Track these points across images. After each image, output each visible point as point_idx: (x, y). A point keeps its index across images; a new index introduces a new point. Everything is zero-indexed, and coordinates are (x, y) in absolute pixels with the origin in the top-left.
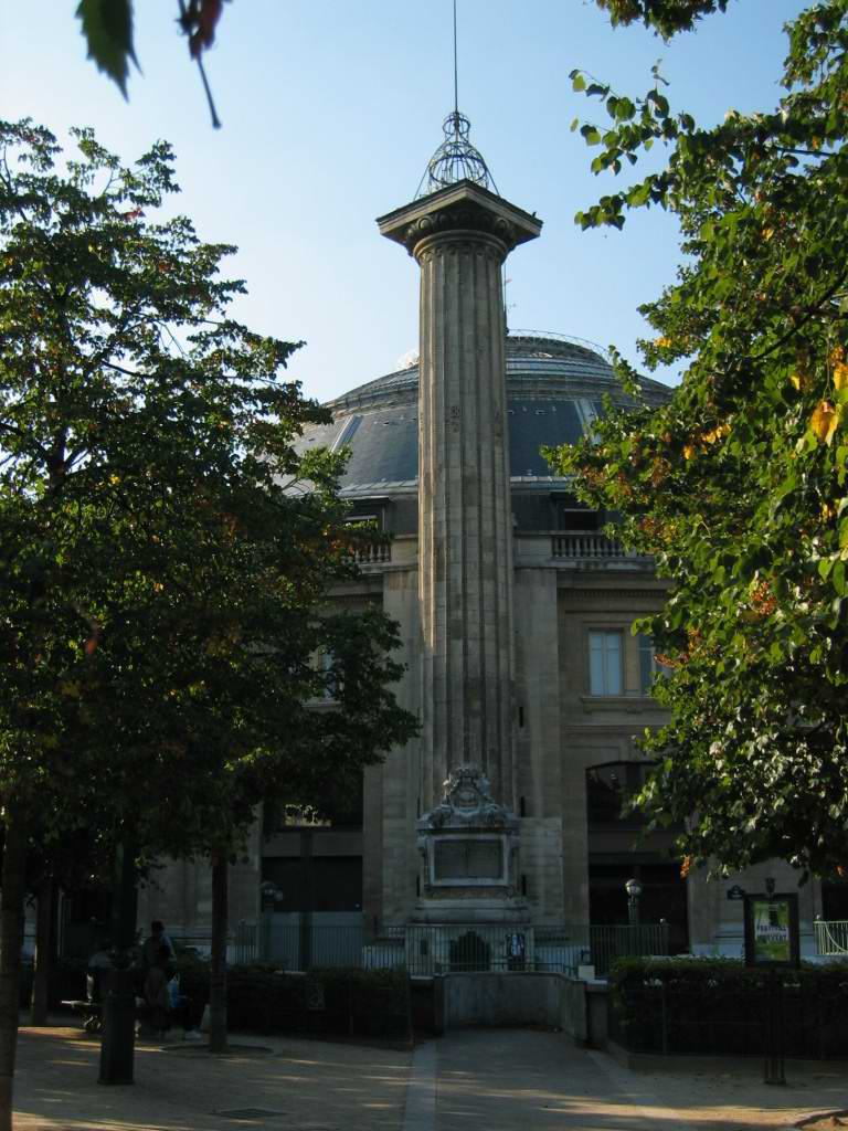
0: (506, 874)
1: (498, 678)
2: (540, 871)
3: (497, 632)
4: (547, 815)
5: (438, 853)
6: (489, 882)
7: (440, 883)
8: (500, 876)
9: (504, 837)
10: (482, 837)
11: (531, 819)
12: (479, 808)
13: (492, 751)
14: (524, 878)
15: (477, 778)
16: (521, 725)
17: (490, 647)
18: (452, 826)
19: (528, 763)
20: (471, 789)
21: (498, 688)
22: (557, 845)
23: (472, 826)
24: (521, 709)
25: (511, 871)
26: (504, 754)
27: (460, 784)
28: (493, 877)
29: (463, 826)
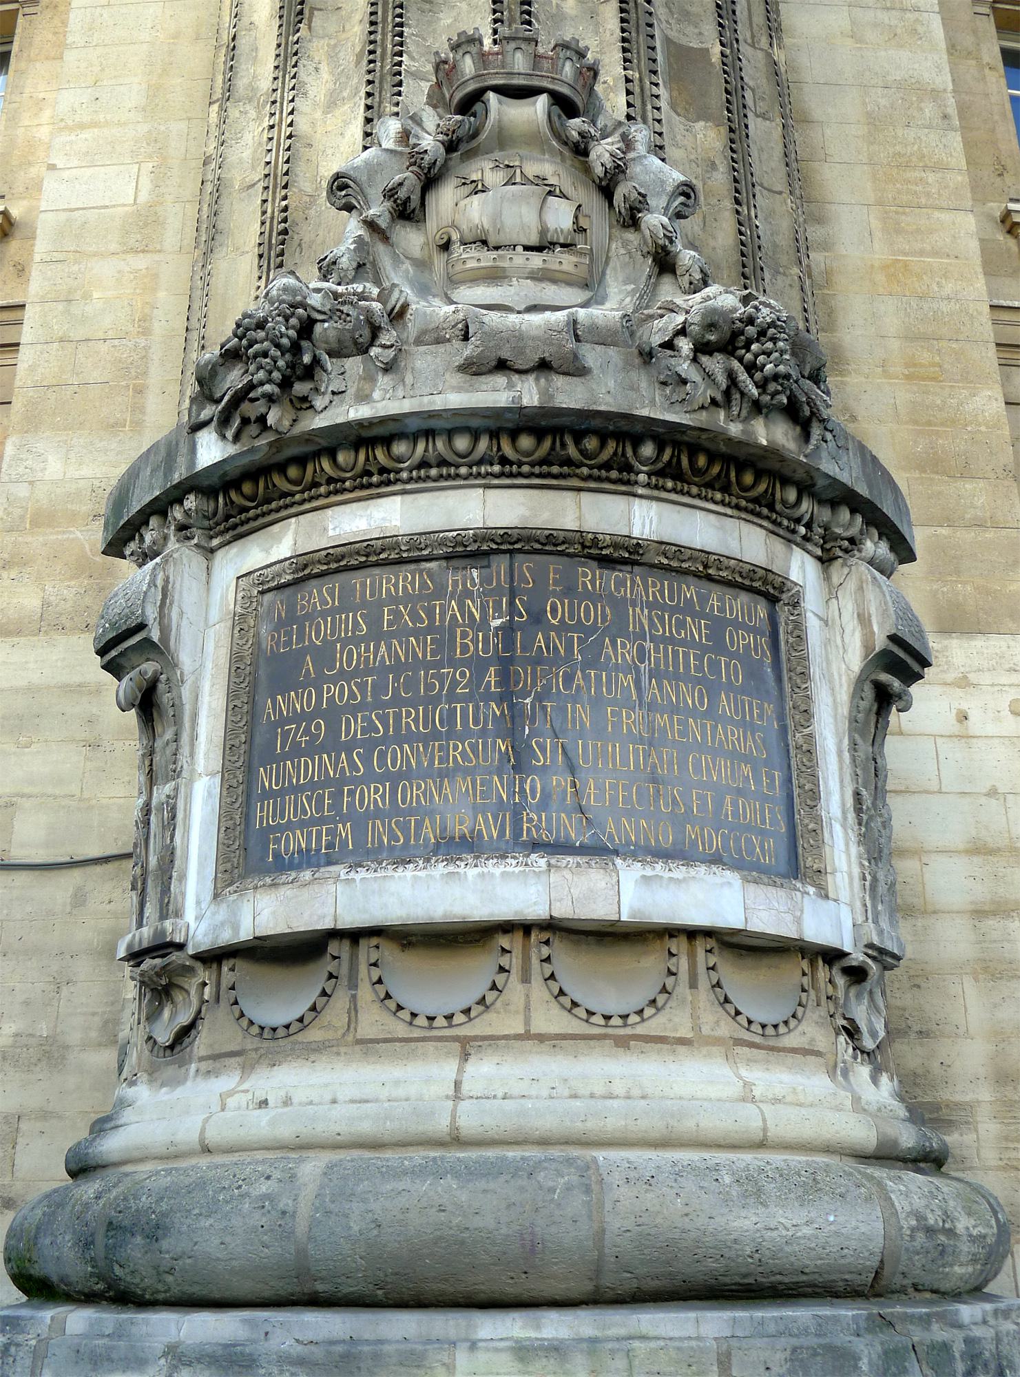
5: (260, 675)
6: (715, 898)
7: (268, 912)
8: (797, 864)
10: (644, 518)
18: (386, 401)
20: (548, 168)
23: (569, 395)
28: (752, 870)
29: (496, 394)
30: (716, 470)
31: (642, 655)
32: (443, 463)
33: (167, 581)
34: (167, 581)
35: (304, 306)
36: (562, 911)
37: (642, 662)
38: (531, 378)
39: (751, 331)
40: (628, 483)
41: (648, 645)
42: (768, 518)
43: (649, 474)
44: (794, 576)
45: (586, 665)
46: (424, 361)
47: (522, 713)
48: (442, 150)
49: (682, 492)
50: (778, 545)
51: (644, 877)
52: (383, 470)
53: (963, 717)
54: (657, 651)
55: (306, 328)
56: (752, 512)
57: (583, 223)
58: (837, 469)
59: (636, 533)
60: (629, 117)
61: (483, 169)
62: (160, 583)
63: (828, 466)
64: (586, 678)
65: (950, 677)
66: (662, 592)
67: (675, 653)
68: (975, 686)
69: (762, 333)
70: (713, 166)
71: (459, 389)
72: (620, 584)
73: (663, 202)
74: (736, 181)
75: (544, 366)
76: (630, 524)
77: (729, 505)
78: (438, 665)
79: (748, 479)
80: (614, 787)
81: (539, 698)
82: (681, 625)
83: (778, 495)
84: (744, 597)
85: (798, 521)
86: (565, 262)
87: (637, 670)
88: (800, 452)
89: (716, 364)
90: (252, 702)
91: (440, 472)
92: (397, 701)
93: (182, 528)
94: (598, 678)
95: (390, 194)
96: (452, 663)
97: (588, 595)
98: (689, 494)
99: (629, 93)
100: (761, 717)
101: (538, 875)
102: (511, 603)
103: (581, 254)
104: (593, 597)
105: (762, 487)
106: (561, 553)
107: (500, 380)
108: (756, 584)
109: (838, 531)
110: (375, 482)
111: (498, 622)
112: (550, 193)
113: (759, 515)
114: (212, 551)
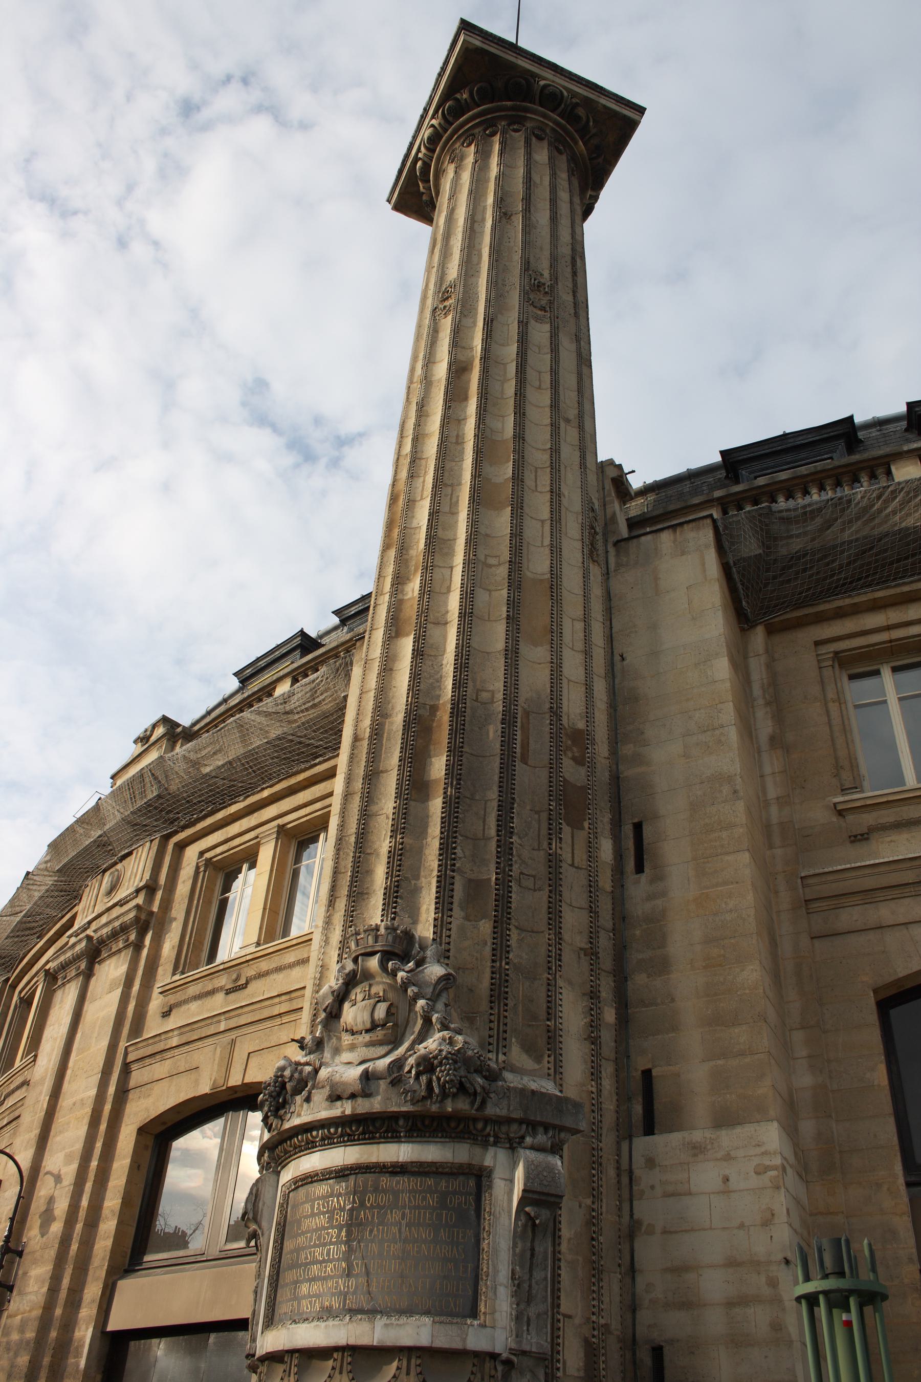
0: (500, 1303)
1: (511, 697)
2: (715, 1322)
3: (513, 604)
4: (725, 1119)
9: (495, 1158)
11: (676, 1137)
12: (401, 1050)
13: (475, 887)
14: (658, 1352)
15: (404, 958)
16: (639, 869)
17: (496, 636)
19: (662, 966)
21: (509, 719)
22: (768, 1221)
23: (363, 1106)
24: (638, 828)
25: (523, 1293)
26: (528, 902)
27: (351, 982)
30: (435, 1124)
31: (403, 1215)
32: (329, 1138)
33: (257, 1190)
34: (257, 1190)
35: (282, 1076)
36: (352, 1341)
37: (403, 1219)
38: (350, 1101)
39: (436, 1062)
40: (397, 1137)
41: (407, 1211)
42: (469, 1138)
43: (406, 1132)
44: (488, 1162)
45: (379, 1224)
46: (319, 1096)
47: (352, 1250)
48: (344, 988)
49: (421, 1137)
50: (478, 1150)
51: (385, 1325)
52: (313, 1142)
53: (726, 1179)
54: (411, 1213)
55: (283, 1085)
56: (460, 1137)
57: (393, 1010)
58: (498, 1110)
59: (401, 1160)
60: (434, 939)
61: (357, 993)
62: (254, 1192)
63: (491, 1110)
64: (378, 1230)
65: (719, 1155)
66: (416, 1184)
67: (419, 1213)
68: (734, 1159)
69: (441, 1064)
70: (486, 944)
71: (325, 1109)
72: (398, 1183)
73: (430, 990)
74: (494, 949)
75: (353, 1096)
76: (398, 1156)
77: (446, 1137)
78: (328, 1228)
79: (453, 1125)
80: (384, 1281)
81: (359, 1242)
82: (424, 1198)
83: (471, 1127)
84: (461, 1178)
85: (489, 1135)
86: (379, 1034)
87: (400, 1223)
88: (472, 1108)
89: (424, 1079)
90: (282, 1243)
91: (328, 1142)
92: (315, 1246)
93: (268, 1163)
94: (383, 1229)
95: (325, 1010)
96: (333, 1227)
97: (384, 1191)
98: (425, 1136)
99: (435, 926)
100: (463, 1237)
101: (344, 1325)
102: (354, 1198)
103: (388, 1029)
104: (384, 1191)
105: (461, 1126)
106: (374, 1172)
107: (339, 1103)
108: (467, 1171)
109: (512, 1135)
110: (310, 1146)
111: (348, 1207)
112: (378, 1001)
113: (464, 1138)
114: (280, 1172)
